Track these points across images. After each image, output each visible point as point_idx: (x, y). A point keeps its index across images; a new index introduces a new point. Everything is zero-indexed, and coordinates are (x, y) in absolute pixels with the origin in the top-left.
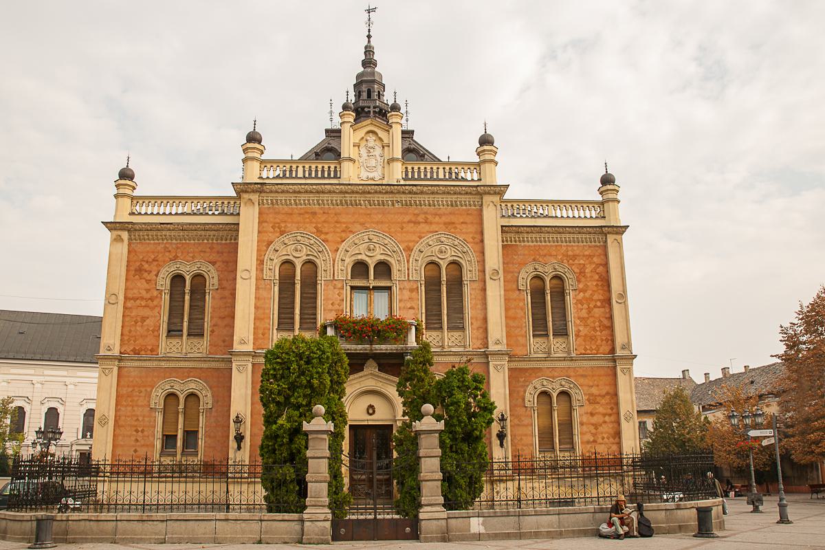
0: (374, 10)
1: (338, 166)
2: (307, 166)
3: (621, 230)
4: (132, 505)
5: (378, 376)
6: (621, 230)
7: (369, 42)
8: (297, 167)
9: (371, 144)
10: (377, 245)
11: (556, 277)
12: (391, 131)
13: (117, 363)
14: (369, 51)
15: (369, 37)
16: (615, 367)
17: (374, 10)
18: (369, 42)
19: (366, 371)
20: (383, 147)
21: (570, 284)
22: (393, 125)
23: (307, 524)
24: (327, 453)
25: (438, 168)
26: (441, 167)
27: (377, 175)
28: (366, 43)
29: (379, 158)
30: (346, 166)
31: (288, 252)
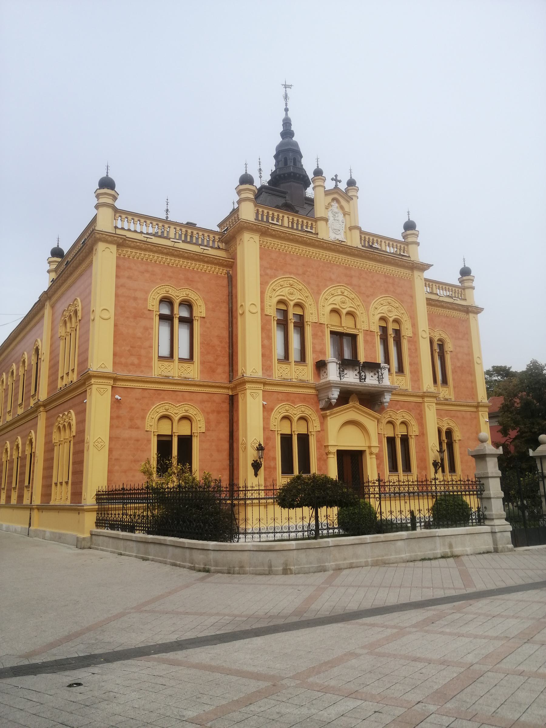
0: (290, 86)
1: (314, 224)
2: (291, 218)
3: (477, 310)
4: (292, 532)
5: (358, 409)
6: (477, 310)
7: (287, 114)
8: (283, 217)
9: (336, 210)
10: (347, 299)
11: (439, 340)
12: (351, 202)
13: (112, 382)
14: (287, 123)
15: (286, 110)
16: (478, 411)
17: (290, 86)
18: (287, 114)
19: (351, 404)
20: (344, 215)
21: (449, 347)
22: (354, 198)
23: (498, 535)
24: (499, 473)
25: (381, 241)
26: (383, 241)
27: (341, 237)
28: (283, 116)
29: (342, 223)
30: (321, 224)
31: (284, 293)
